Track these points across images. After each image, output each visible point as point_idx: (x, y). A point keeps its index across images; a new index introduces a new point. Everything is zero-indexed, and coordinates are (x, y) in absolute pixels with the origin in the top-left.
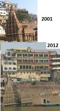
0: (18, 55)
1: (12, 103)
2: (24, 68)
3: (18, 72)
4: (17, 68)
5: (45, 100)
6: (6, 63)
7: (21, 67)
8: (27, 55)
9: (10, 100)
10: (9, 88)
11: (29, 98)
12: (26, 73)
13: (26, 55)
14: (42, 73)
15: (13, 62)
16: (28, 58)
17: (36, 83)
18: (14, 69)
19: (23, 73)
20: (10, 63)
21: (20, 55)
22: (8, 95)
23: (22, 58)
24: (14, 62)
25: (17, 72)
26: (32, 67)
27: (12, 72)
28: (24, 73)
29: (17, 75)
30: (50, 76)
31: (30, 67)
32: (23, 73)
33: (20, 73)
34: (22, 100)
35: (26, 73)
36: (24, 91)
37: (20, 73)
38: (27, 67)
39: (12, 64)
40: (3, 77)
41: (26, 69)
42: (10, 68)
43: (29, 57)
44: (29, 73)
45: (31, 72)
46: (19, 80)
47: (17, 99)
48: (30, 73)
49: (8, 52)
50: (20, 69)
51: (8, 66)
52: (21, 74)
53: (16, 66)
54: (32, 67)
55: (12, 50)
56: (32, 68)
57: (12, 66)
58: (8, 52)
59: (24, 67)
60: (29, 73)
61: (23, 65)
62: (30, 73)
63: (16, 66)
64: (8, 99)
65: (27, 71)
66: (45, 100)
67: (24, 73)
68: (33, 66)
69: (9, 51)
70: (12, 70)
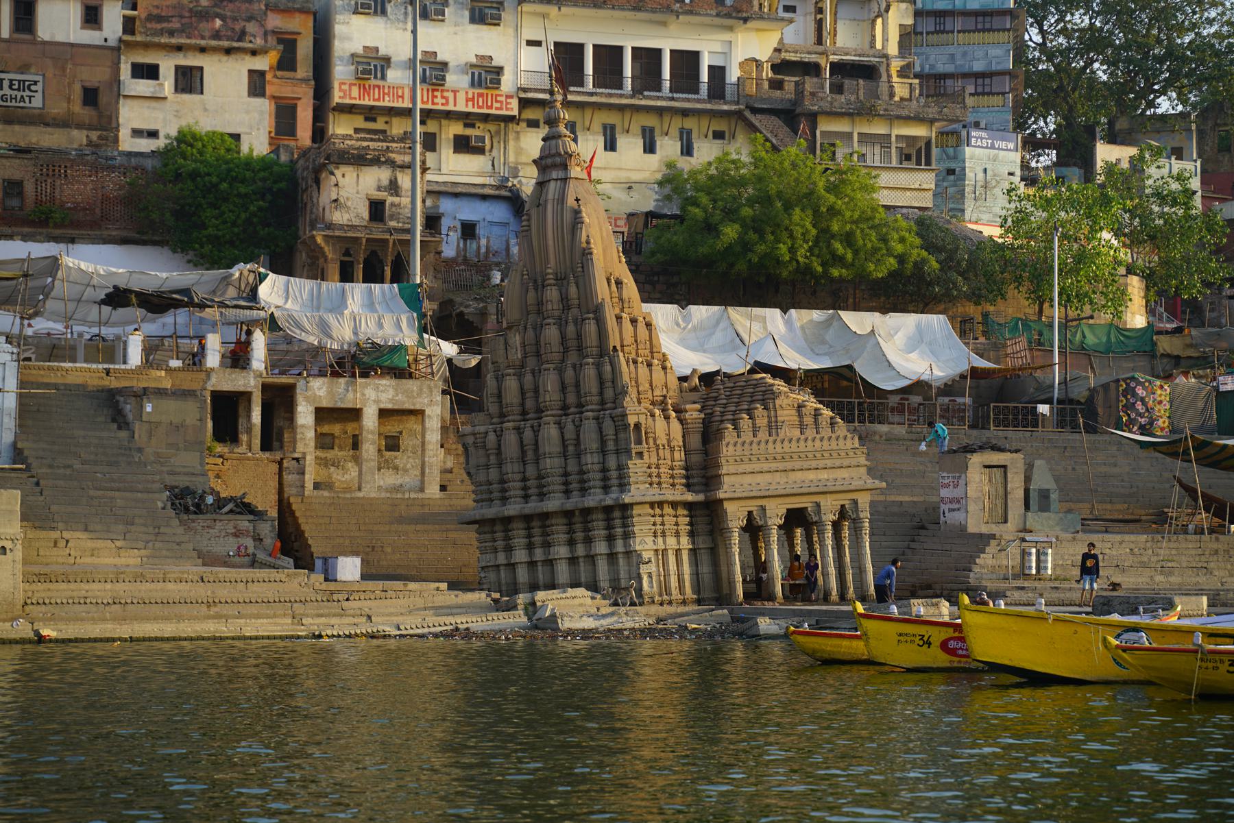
7: (567, 59)
10: (561, 280)
28: (611, 146)
30: (926, 201)
40: (376, 162)
42: (433, 71)
56: (704, 76)
59: (609, 57)
65: (650, 121)
67: (611, 146)
70: (459, 93)
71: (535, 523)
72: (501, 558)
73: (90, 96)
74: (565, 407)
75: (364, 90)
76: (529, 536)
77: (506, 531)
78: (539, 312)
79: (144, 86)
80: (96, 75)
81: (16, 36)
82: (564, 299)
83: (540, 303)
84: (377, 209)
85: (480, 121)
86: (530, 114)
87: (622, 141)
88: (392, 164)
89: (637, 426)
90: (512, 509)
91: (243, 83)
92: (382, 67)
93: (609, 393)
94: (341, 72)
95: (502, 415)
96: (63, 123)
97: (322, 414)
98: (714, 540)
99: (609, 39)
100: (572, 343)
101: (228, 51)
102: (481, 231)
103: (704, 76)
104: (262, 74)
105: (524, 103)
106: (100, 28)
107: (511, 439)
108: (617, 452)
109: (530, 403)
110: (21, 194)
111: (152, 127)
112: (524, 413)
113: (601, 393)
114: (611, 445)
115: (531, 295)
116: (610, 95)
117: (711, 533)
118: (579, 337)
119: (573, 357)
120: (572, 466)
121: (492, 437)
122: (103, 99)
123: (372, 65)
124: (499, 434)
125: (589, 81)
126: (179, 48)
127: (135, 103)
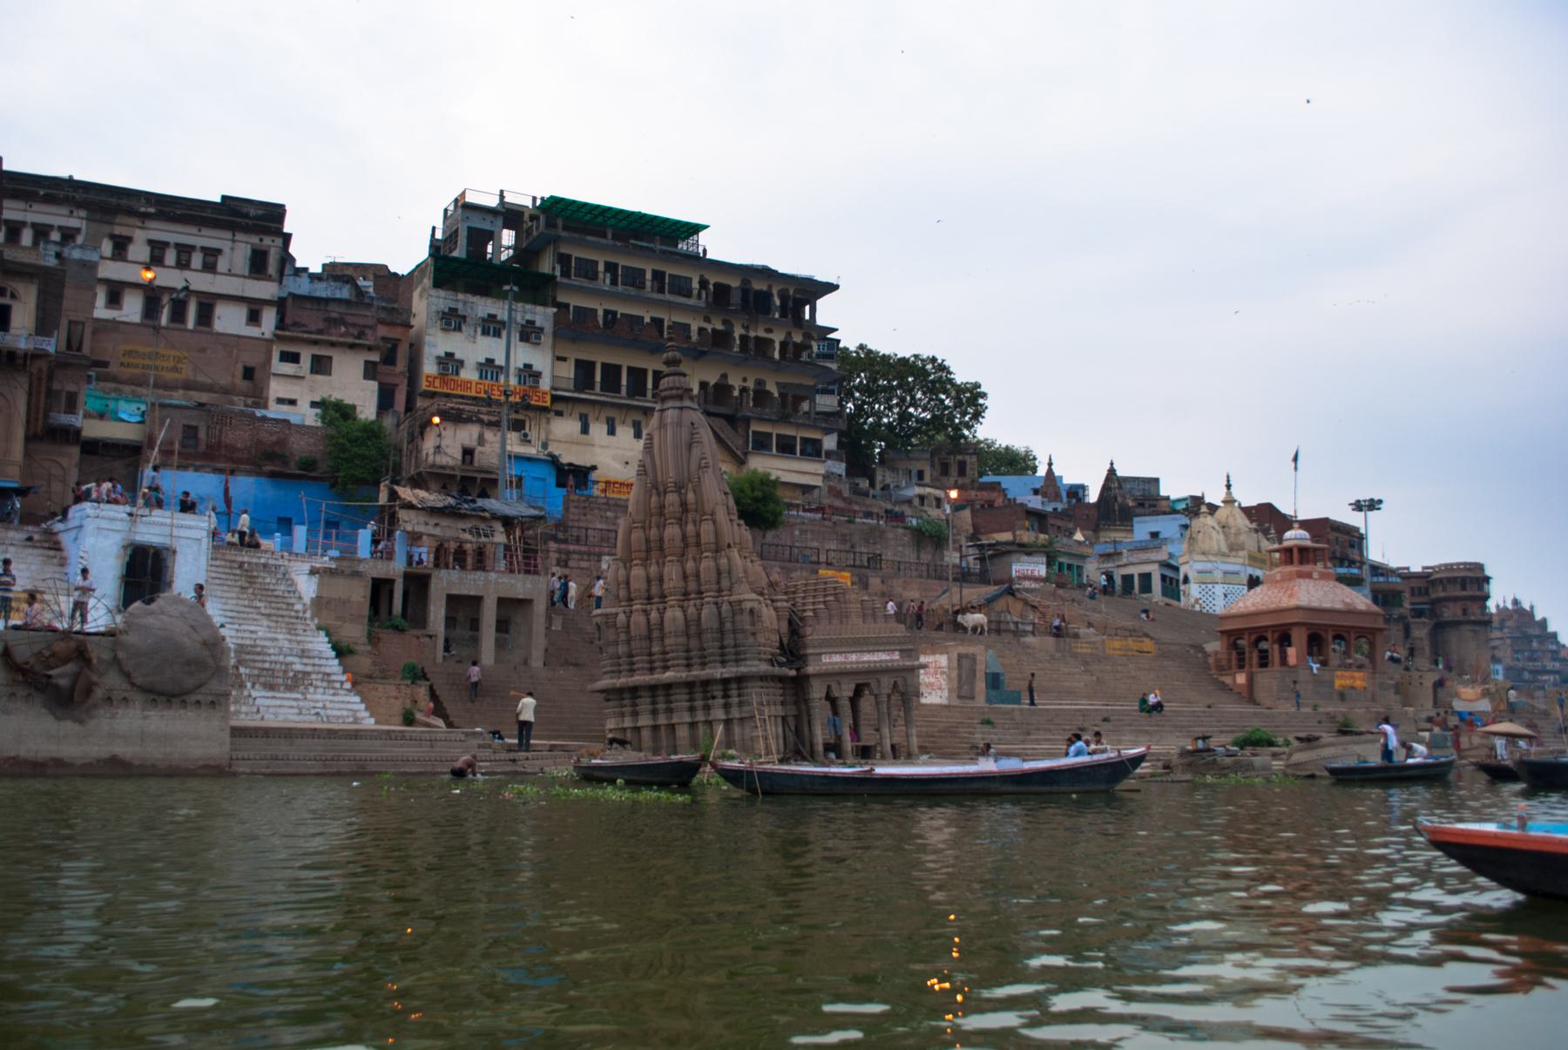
1: (723, 663)
3: (559, 414)
6: (452, 320)
7: (584, 368)
9: (692, 628)
10: (679, 488)
14: (762, 444)
15: (519, 319)
19: (598, 430)
20: (491, 326)
22: (672, 572)
24: (532, 323)
28: (612, 432)
32: (598, 430)
40: (468, 420)
41: (631, 395)
43: (660, 296)
49: (470, 229)
50: (577, 389)
51: (474, 349)
58: (470, 229)
59: (611, 372)
61: (600, 357)
63: (540, 359)
64: (674, 615)
67: (612, 432)
71: (660, 692)
72: (628, 723)
73: (249, 373)
74: (686, 594)
75: (444, 383)
76: (654, 703)
77: (634, 698)
78: (661, 514)
79: (288, 368)
80: (252, 359)
82: (684, 504)
83: (662, 507)
84: (468, 453)
86: (559, 407)
88: (480, 421)
89: (752, 611)
90: (640, 679)
93: (725, 583)
94: (429, 368)
95: (630, 599)
97: (454, 601)
98: (799, 709)
99: (612, 360)
100: (692, 540)
101: (352, 346)
102: (527, 483)
104: (374, 363)
105: (555, 399)
107: (638, 620)
108: (734, 632)
109: (654, 590)
110: (195, 436)
111: (292, 397)
112: (649, 598)
113: (718, 582)
114: (728, 626)
115: (654, 499)
117: (796, 703)
118: (698, 535)
119: (692, 551)
120: (694, 643)
121: (622, 617)
122: (257, 375)
124: (629, 615)
126: (316, 343)
127: (282, 380)
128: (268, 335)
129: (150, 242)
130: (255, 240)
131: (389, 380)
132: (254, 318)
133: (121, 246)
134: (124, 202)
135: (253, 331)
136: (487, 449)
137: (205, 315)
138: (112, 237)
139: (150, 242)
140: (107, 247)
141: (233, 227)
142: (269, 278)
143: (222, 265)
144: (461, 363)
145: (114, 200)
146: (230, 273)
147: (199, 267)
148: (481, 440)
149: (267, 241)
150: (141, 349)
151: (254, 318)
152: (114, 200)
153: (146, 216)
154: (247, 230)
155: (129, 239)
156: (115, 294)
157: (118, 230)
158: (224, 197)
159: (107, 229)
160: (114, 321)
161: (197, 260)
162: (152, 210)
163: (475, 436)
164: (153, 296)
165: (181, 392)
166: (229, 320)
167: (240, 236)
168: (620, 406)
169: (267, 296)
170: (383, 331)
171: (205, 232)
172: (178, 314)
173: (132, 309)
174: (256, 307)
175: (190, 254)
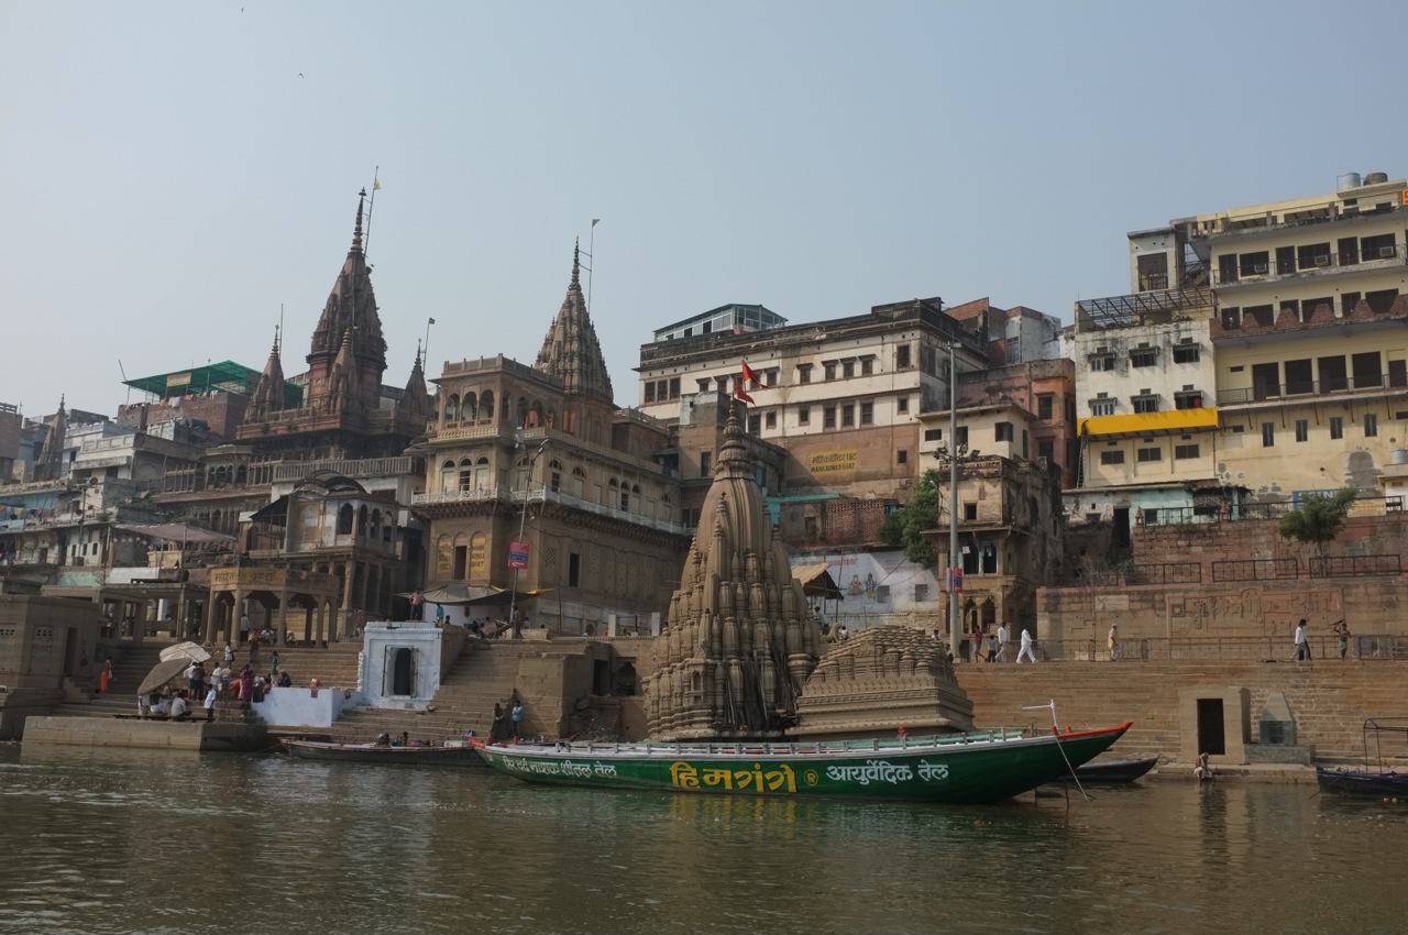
0: (1227, 261)
2: (1288, 391)
3: (1239, 429)
4: (1218, 392)
5: (1210, 713)
6: (1105, 360)
8: (1325, 248)
11: (906, 675)
12: (1319, 436)
13: (1313, 255)
16: (1331, 285)
17: (1338, 523)
18: (1189, 400)
19: (1285, 439)
20: (1144, 358)
21: (1255, 262)
23: (1270, 291)
25: (1218, 434)
26: (1391, 364)
27: (1167, 433)
28: (1301, 437)
29: (1220, 455)
31: (1367, 367)
32: (1285, 439)
33: (1252, 440)
34: (811, 691)
35: (1319, 436)
36: (1168, 613)
37: (1252, 440)
38: (1333, 367)
39: (1160, 360)
41: (1324, 391)
44: (1354, 434)
45: (1381, 414)
46: (1215, 500)
47: (751, 683)
48: (1370, 431)
51: (1125, 384)
52: (1268, 441)
53: (1201, 376)
54: (1391, 364)
55: (1180, 232)
56: (1385, 370)
57: (1166, 380)
59: (1298, 372)
60: (1354, 434)
61: (1281, 356)
62: (1370, 431)
63: (1201, 376)
66: (1210, 713)
67: (1301, 437)
68: (1395, 357)
69: (1148, 242)
70: (1170, 417)
73: (903, 457)
80: (901, 445)
81: (844, 429)
84: (971, 510)
85: (1194, 433)
87: (1278, 437)
91: (993, 431)
92: (1111, 406)
94: (1083, 413)
96: (889, 476)
103: (1385, 370)
106: (908, 413)
116: (1304, 397)
122: (909, 457)
123: (1103, 404)
125: (1283, 389)
128: (915, 420)
129: (824, 363)
130: (898, 337)
131: (1046, 433)
132: (903, 407)
133: (805, 370)
134: (805, 336)
135: (903, 419)
136: (988, 501)
137: (867, 416)
138: (799, 366)
139: (824, 363)
140: (797, 375)
141: (881, 333)
142: (913, 369)
143: (876, 367)
144: (1115, 400)
145: (798, 337)
146: (883, 373)
147: (860, 374)
148: (982, 494)
149: (908, 335)
150: (825, 455)
151: (903, 407)
152: (798, 337)
153: (821, 342)
154: (892, 331)
155: (810, 366)
156: (804, 411)
157: (803, 360)
158: (874, 309)
159: (795, 361)
160: (805, 435)
161: (858, 368)
162: (824, 336)
163: (976, 491)
164: (829, 406)
165: (854, 484)
166: (884, 413)
167: (888, 338)
168: (1314, 406)
169: (912, 386)
170: (1037, 388)
171: (863, 342)
172: (848, 420)
173: (817, 419)
174: (903, 397)
175: (834, 366)
